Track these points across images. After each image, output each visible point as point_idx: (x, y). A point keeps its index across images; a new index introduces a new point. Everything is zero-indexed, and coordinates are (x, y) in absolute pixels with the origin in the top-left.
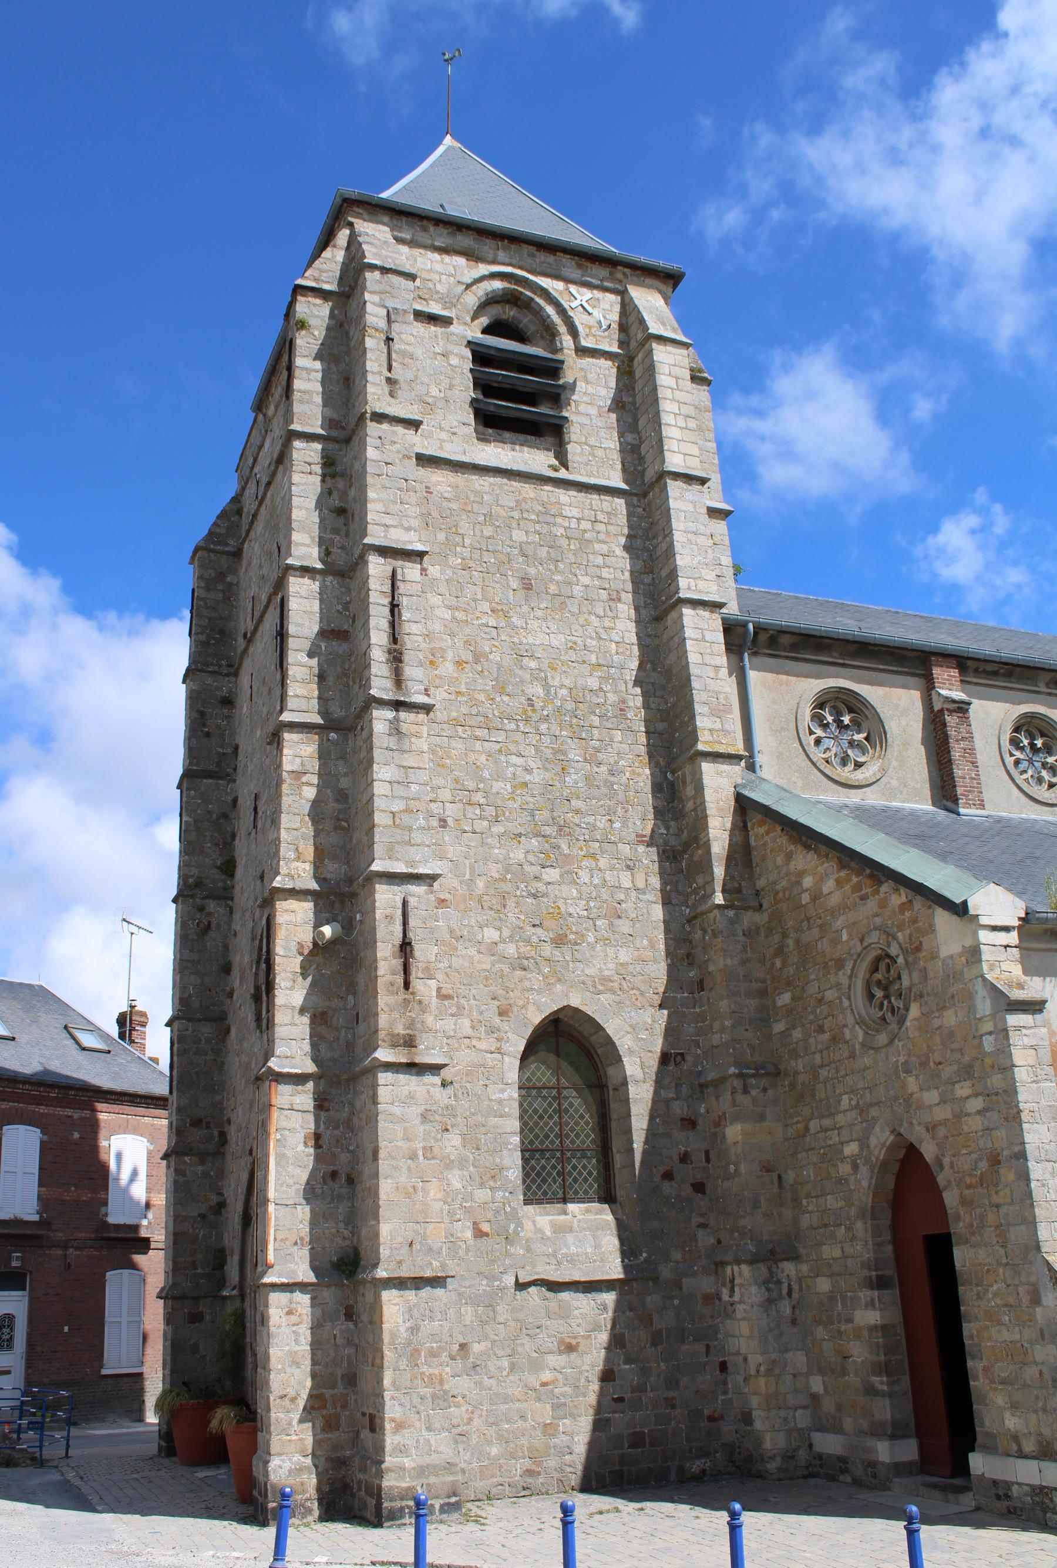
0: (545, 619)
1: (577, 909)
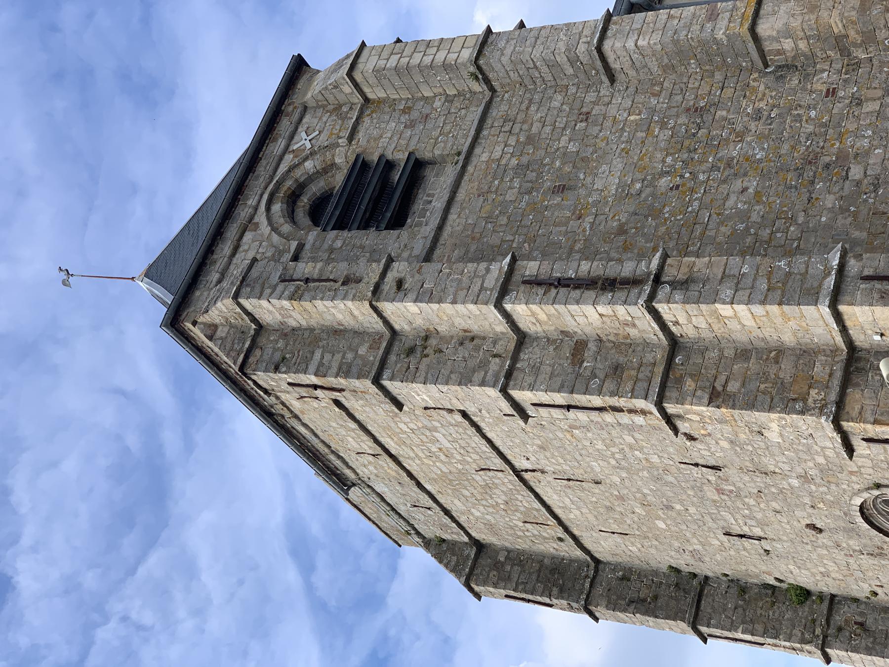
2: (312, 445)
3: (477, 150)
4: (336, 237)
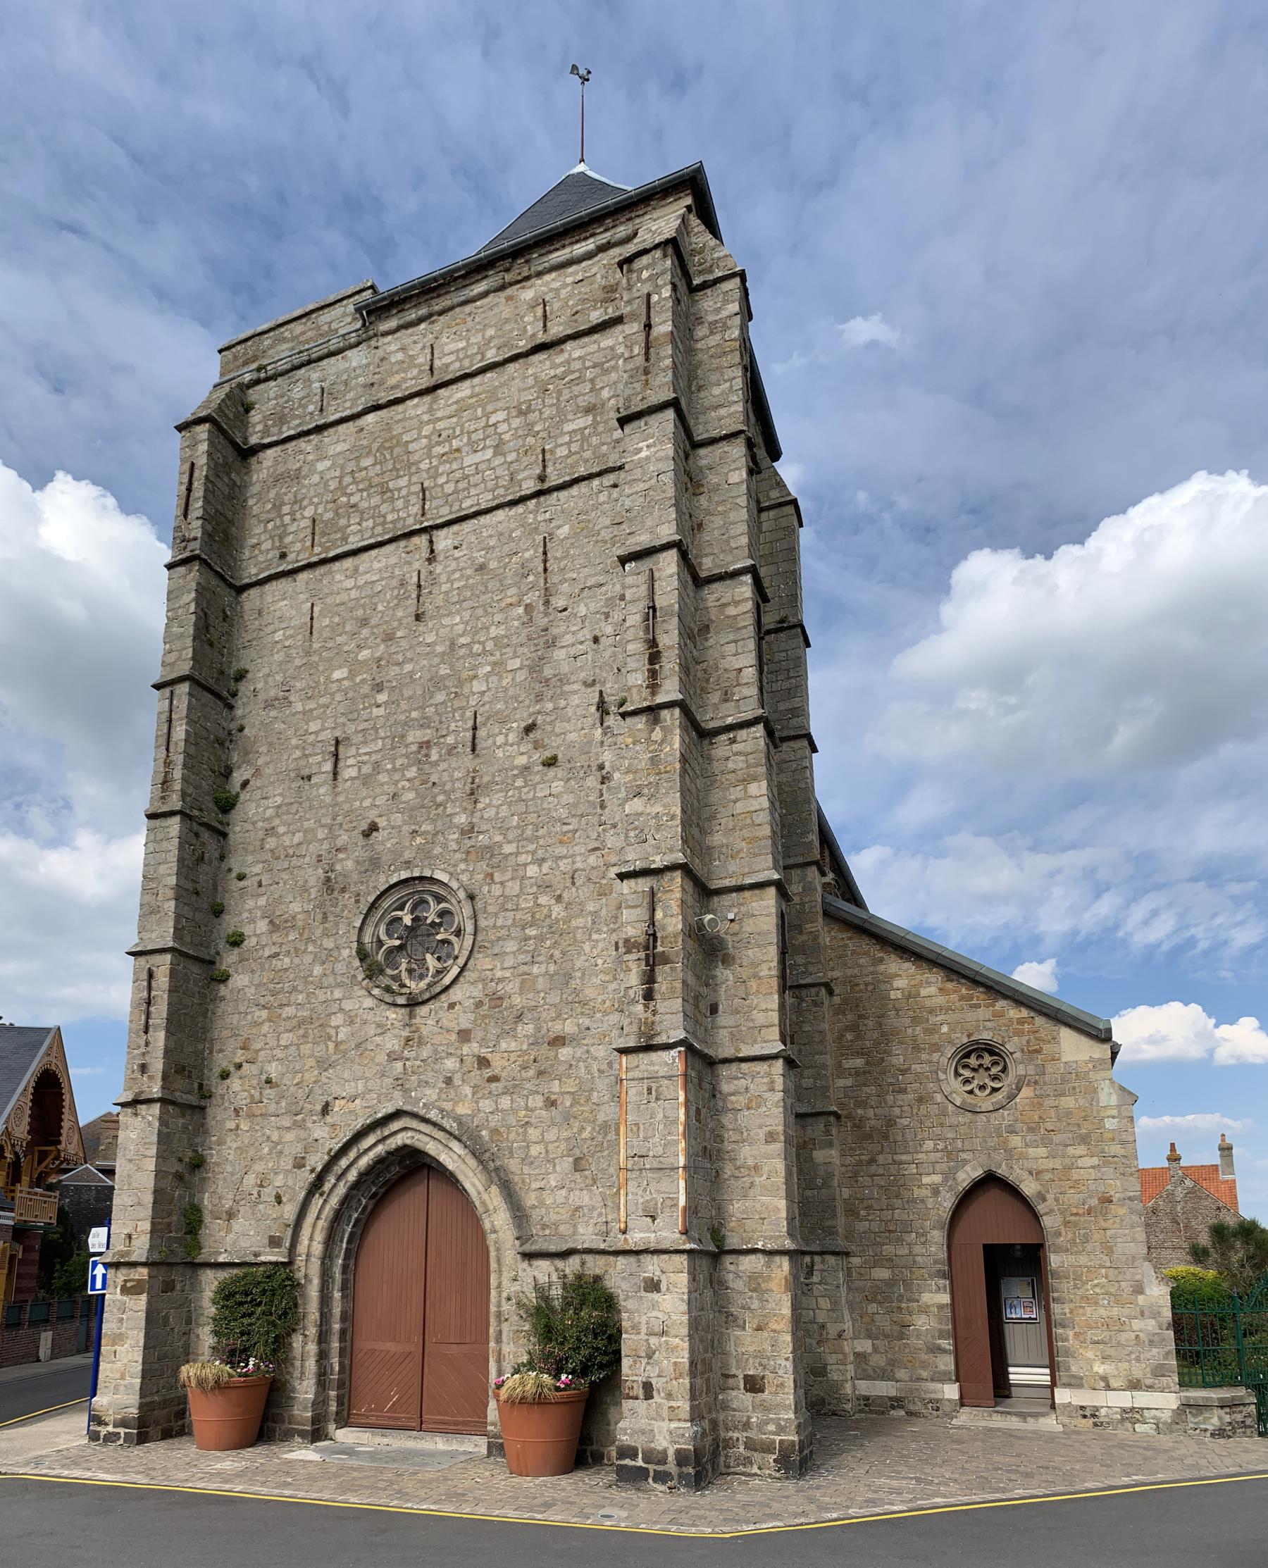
2: (449, 292)
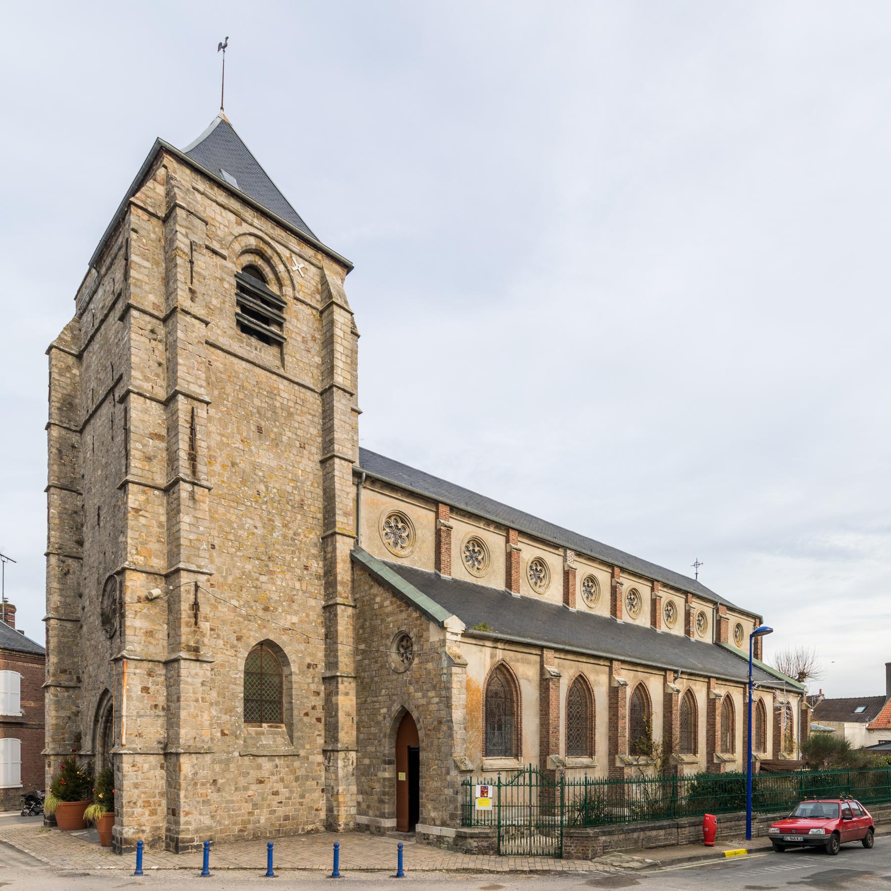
0: (268, 451)
1: (275, 597)
3: (286, 382)
4: (231, 284)
